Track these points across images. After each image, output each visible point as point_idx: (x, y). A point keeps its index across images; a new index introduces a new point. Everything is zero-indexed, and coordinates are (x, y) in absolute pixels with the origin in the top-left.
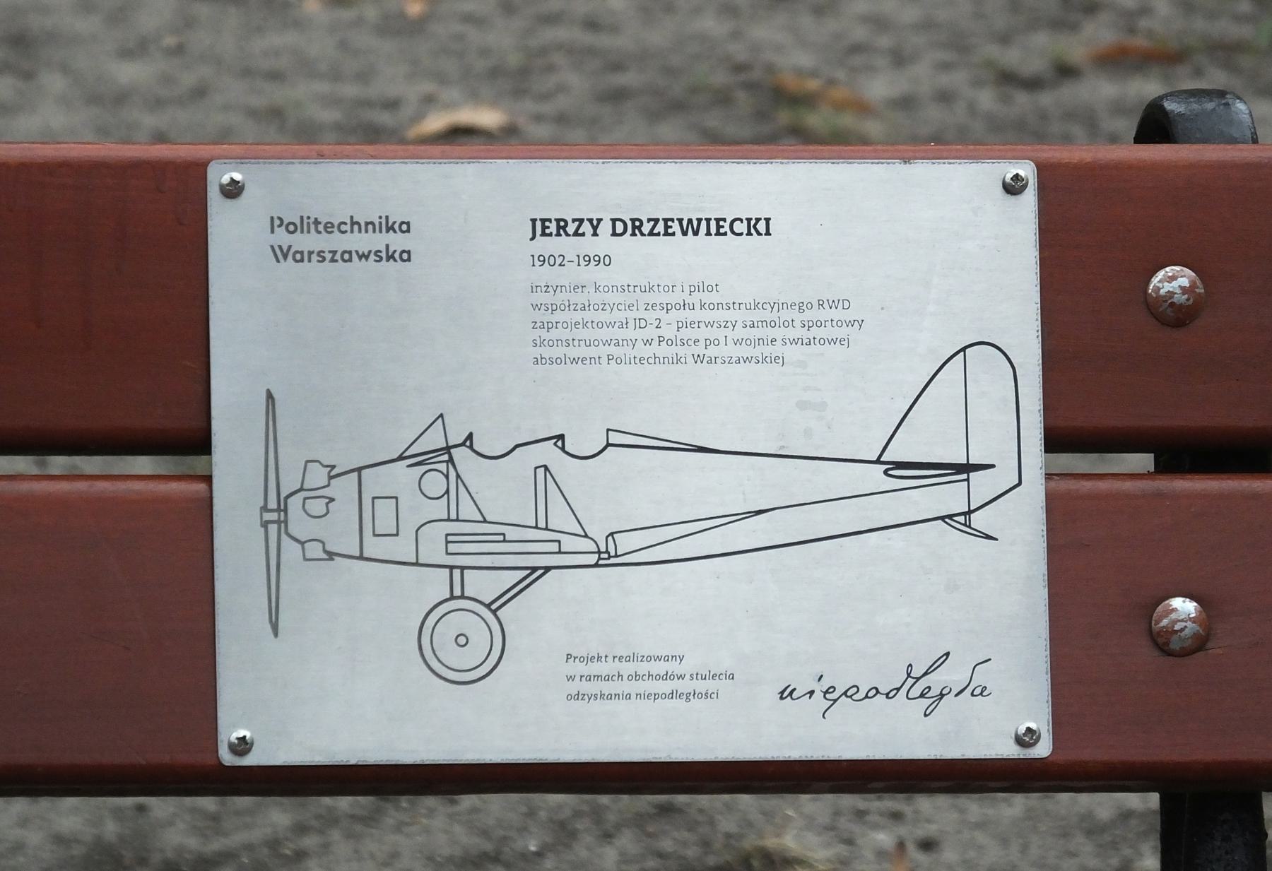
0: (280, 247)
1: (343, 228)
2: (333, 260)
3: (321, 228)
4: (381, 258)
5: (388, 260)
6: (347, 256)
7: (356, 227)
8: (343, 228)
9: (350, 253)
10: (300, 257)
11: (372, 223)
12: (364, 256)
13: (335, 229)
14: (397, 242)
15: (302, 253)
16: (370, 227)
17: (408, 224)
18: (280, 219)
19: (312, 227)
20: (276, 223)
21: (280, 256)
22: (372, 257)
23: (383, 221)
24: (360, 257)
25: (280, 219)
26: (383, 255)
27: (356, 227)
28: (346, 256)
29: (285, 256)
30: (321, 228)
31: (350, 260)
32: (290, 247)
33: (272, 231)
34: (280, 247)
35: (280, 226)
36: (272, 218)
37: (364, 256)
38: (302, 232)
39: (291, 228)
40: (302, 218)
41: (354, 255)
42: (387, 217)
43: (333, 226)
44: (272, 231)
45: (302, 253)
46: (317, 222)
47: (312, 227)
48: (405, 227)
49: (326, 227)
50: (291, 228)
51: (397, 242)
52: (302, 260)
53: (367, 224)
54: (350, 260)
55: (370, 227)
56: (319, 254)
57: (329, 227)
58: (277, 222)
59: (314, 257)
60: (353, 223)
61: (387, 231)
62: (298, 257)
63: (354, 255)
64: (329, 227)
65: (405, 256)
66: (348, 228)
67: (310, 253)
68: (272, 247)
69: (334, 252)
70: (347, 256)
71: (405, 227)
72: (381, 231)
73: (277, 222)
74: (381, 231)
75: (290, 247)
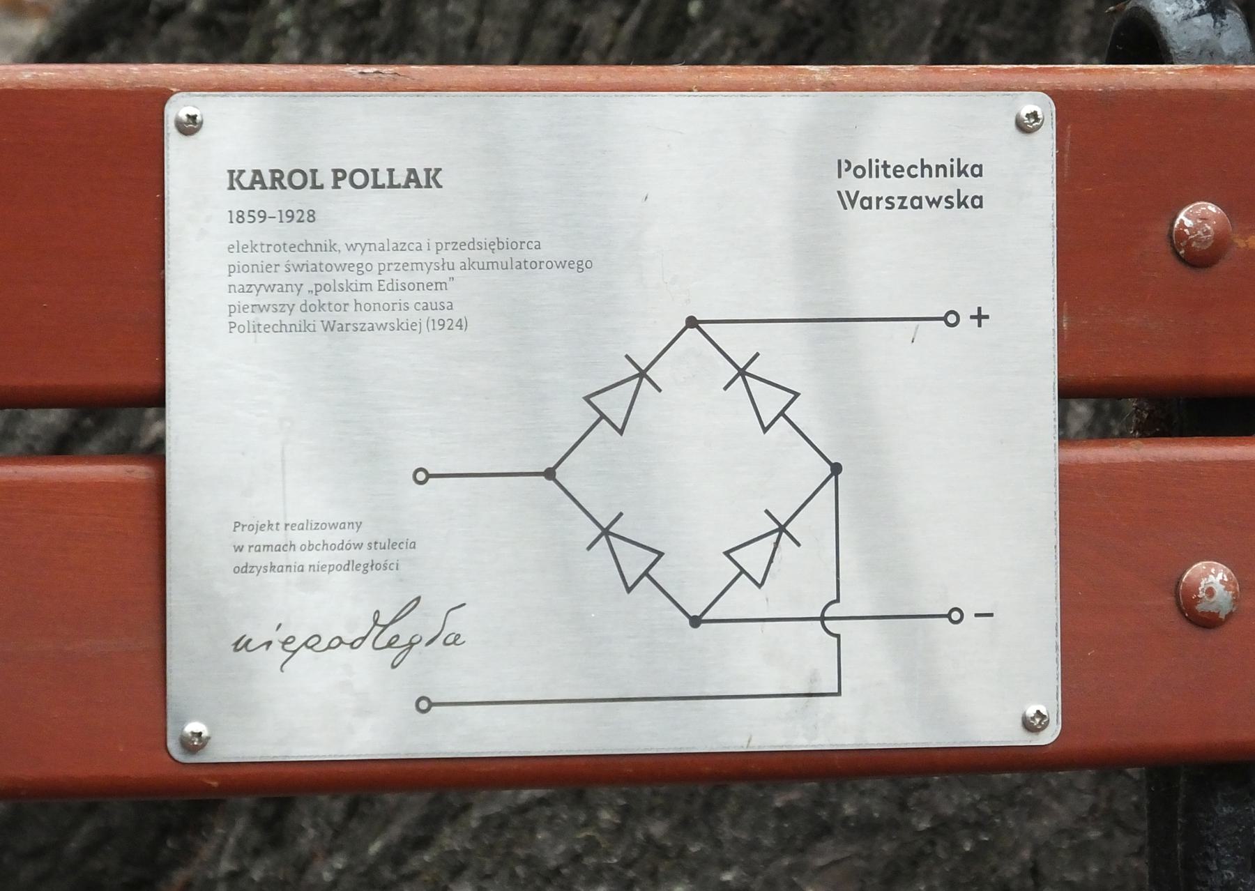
0: (848, 193)
1: (913, 171)
2: (901, 207)
3: (890, 171)
4: (952, 204)
5: (959, 207)
6: (917, 203)
7: (926, 170)
8: (913, 171)
9: (920, 199)
10: (868, 203)
11: (944, 166)
12: (934, 203)
13: (905, 173)
14: (969, 186)
15: (870, 199)
16: (941, 170)
17: (980, 167)
18: (847, 161)
19: (881, 171)
20: (843, 166)
21: (848, 204)
22: (943, 202)
23: (955, 163)
24: (931, 205)
25: (847, 161)
26: (955, 201)
27: (926, 170)
28: (916, 203)
29: (853, 203)
30: (890, 171)
31: (920, 207)
32: (857, 193)
33: (840, 176)
34: (848, 193)
35: (847, 170)
36: (840, 162)
37: (934, 203)
38: (871, 176)
39: (859, 172)
40: (870, 161)
41: (924, 201)
42: (959, 160)
43: (903, 170)
44: (840, 176)
45: (870, 199)
46: (886, 166)
47: (881, 171)
48: (978, 171)
49: (895, 171)
50: (859, 172)
51: (969, 186)
52: (870, 207)
53: (938, 167)
54: (920, 207)
55: (941, 170)
56: (887, 201)
57: (898, 171)
58: (844, 166)
59: (883, 204)
60: (923, 167)
61: (959, 175)
62: (866, 203)
63: (924, 201)
64: (898, 171)
65: (977, 202)
66: (918, 171)
67: (879, 199)
68: (839, 193)
69: (904, 198)
70: (917, 203)
71: (978, 171)
72: (952, 175)
73: (844, 166)
74: (952, 175)
75: (857, 193)
